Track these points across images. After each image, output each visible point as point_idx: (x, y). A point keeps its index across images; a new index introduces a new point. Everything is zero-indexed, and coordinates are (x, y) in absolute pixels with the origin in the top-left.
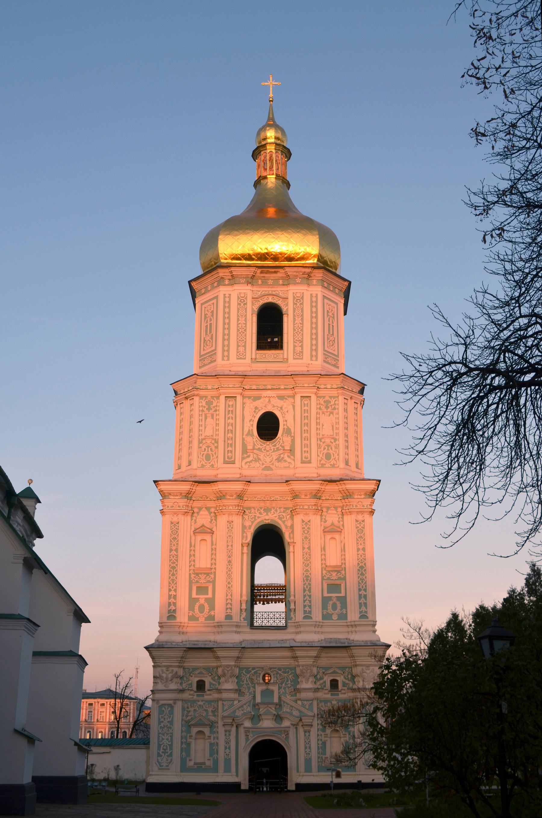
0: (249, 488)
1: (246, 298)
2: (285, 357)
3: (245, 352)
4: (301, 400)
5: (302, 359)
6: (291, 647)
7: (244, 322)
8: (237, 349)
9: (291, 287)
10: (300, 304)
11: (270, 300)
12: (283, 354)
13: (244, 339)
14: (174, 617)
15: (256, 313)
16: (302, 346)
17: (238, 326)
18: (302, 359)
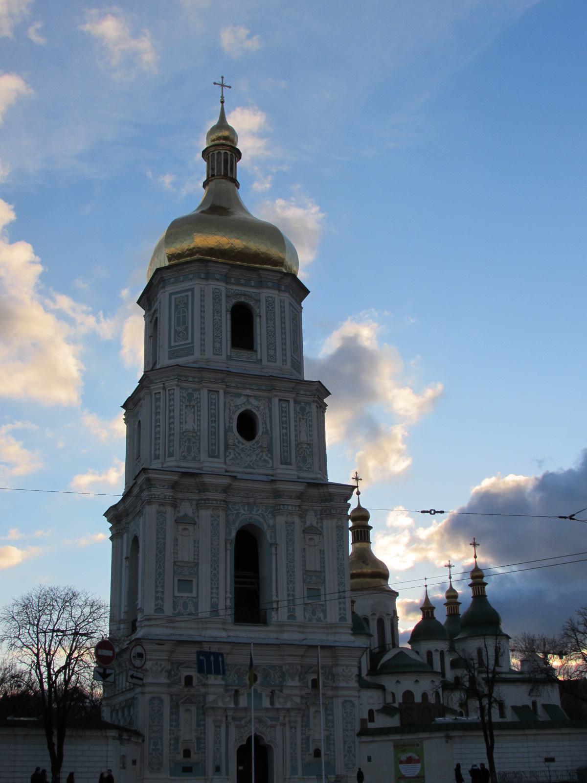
0: (234, 484)
1: (221, 294)
2: (259, 357)
3: (221, 349)
4: (279, 402)
5: (276, 362)
6: (281, 644)
7: (220, 318)
8: (214, 345)
9: (264, 290)
10: (272, 308)
11: (243, 299)
12: (257, 356)
13: (219, 335)
14: (162, 611)
15: (230, 310)
16: (275, 350)
17: (214, 322)
18: (276, 362)
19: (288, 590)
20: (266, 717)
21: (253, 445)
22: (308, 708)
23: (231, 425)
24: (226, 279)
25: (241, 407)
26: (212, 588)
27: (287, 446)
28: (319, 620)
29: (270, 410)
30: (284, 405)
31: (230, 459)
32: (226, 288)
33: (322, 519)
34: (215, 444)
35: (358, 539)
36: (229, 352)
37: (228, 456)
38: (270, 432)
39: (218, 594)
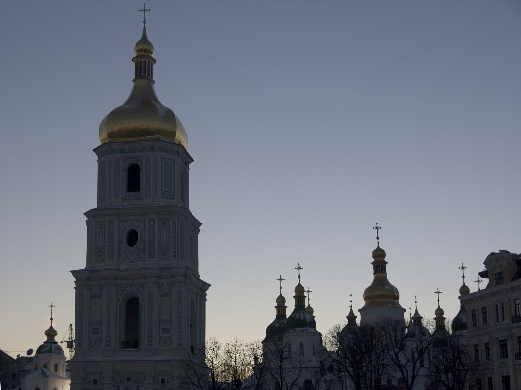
4: (149, 222)
5: (150, 197)
11: (133, 162)
18: (150, 197)
21: (135, 249)
23: (122, 239)
24: (123, 151)
25: (128, 227)
31: (122, 259)
35: (377, 271)
37: (120, 257)
38: (144, 240)
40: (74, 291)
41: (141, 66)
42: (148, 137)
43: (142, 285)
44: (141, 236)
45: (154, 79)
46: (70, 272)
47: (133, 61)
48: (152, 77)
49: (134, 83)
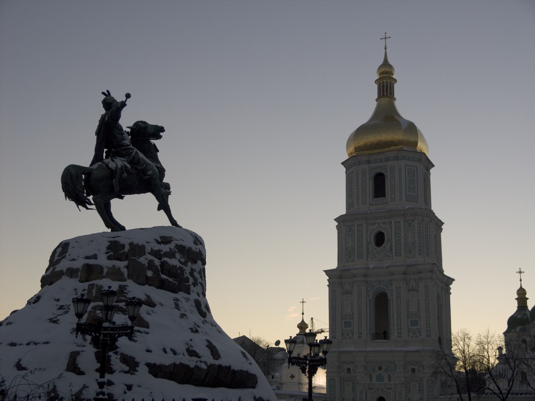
3: (366, 201)
4: (395, 224)
11: (378, 171)
12: (386, 200)
18: (395, 201)
19: (398, 323)
20: (386, 388)
21: (382, 249)
22: (410, 383)
24: (369, 162)
26: (359, 325)
27: (399, 247)
28: (417, 337)
29: (391, 228)
30: (398, 224)
31: (370, 258)
32: (369, 167)
33: (418, 283)
34: (361, 253)
36: (371, 201)
39: (361, 328)
40: (328, 288)
41: (383, 87)
42: (392, 148)
43: (390, 281)
44: (388, 237)
45: (395, 96)
46: (324, 272)
47: (375, 83)
48: (393, 95)
49: (377, 101)
